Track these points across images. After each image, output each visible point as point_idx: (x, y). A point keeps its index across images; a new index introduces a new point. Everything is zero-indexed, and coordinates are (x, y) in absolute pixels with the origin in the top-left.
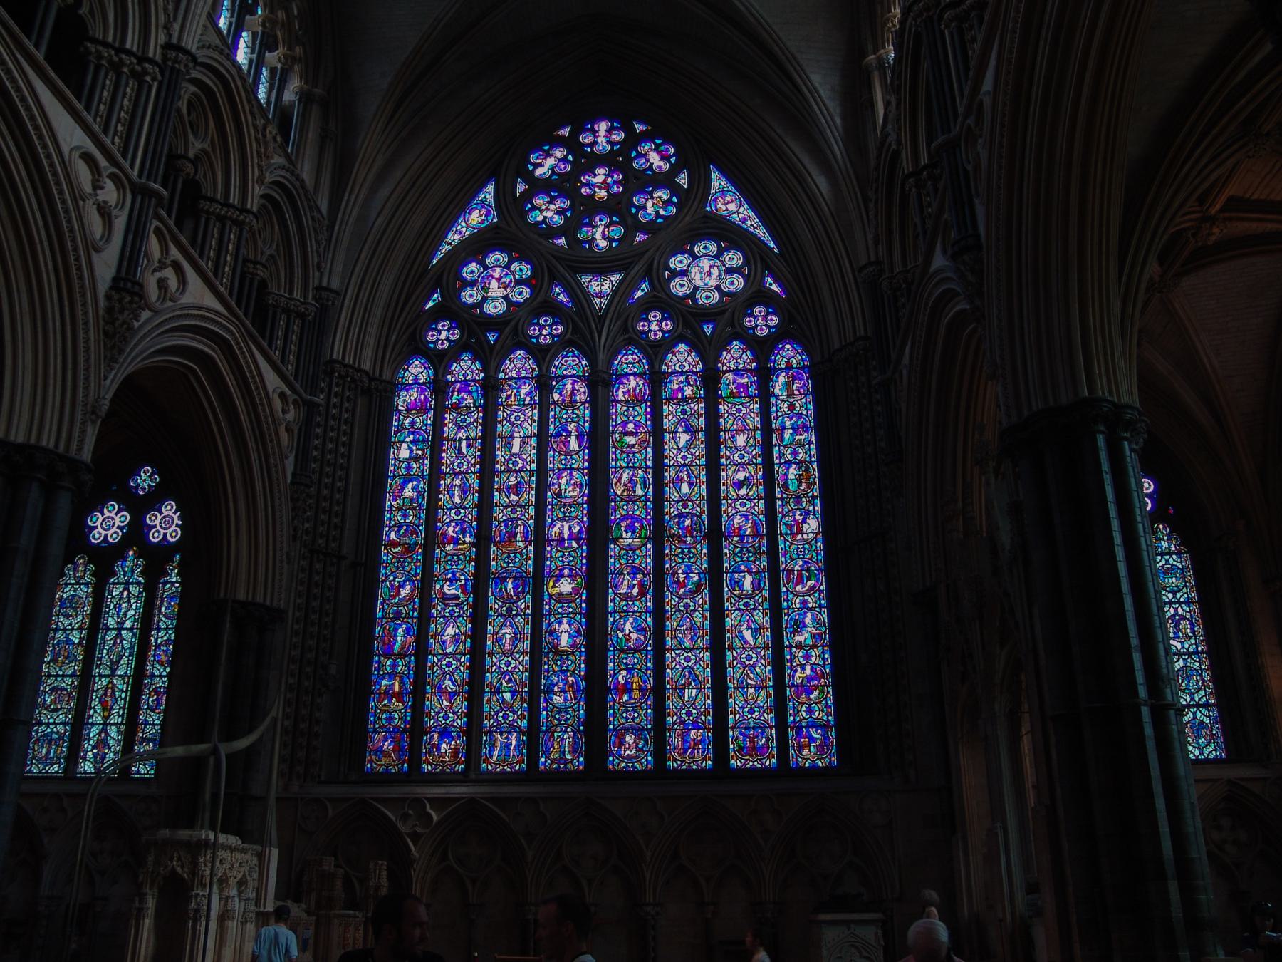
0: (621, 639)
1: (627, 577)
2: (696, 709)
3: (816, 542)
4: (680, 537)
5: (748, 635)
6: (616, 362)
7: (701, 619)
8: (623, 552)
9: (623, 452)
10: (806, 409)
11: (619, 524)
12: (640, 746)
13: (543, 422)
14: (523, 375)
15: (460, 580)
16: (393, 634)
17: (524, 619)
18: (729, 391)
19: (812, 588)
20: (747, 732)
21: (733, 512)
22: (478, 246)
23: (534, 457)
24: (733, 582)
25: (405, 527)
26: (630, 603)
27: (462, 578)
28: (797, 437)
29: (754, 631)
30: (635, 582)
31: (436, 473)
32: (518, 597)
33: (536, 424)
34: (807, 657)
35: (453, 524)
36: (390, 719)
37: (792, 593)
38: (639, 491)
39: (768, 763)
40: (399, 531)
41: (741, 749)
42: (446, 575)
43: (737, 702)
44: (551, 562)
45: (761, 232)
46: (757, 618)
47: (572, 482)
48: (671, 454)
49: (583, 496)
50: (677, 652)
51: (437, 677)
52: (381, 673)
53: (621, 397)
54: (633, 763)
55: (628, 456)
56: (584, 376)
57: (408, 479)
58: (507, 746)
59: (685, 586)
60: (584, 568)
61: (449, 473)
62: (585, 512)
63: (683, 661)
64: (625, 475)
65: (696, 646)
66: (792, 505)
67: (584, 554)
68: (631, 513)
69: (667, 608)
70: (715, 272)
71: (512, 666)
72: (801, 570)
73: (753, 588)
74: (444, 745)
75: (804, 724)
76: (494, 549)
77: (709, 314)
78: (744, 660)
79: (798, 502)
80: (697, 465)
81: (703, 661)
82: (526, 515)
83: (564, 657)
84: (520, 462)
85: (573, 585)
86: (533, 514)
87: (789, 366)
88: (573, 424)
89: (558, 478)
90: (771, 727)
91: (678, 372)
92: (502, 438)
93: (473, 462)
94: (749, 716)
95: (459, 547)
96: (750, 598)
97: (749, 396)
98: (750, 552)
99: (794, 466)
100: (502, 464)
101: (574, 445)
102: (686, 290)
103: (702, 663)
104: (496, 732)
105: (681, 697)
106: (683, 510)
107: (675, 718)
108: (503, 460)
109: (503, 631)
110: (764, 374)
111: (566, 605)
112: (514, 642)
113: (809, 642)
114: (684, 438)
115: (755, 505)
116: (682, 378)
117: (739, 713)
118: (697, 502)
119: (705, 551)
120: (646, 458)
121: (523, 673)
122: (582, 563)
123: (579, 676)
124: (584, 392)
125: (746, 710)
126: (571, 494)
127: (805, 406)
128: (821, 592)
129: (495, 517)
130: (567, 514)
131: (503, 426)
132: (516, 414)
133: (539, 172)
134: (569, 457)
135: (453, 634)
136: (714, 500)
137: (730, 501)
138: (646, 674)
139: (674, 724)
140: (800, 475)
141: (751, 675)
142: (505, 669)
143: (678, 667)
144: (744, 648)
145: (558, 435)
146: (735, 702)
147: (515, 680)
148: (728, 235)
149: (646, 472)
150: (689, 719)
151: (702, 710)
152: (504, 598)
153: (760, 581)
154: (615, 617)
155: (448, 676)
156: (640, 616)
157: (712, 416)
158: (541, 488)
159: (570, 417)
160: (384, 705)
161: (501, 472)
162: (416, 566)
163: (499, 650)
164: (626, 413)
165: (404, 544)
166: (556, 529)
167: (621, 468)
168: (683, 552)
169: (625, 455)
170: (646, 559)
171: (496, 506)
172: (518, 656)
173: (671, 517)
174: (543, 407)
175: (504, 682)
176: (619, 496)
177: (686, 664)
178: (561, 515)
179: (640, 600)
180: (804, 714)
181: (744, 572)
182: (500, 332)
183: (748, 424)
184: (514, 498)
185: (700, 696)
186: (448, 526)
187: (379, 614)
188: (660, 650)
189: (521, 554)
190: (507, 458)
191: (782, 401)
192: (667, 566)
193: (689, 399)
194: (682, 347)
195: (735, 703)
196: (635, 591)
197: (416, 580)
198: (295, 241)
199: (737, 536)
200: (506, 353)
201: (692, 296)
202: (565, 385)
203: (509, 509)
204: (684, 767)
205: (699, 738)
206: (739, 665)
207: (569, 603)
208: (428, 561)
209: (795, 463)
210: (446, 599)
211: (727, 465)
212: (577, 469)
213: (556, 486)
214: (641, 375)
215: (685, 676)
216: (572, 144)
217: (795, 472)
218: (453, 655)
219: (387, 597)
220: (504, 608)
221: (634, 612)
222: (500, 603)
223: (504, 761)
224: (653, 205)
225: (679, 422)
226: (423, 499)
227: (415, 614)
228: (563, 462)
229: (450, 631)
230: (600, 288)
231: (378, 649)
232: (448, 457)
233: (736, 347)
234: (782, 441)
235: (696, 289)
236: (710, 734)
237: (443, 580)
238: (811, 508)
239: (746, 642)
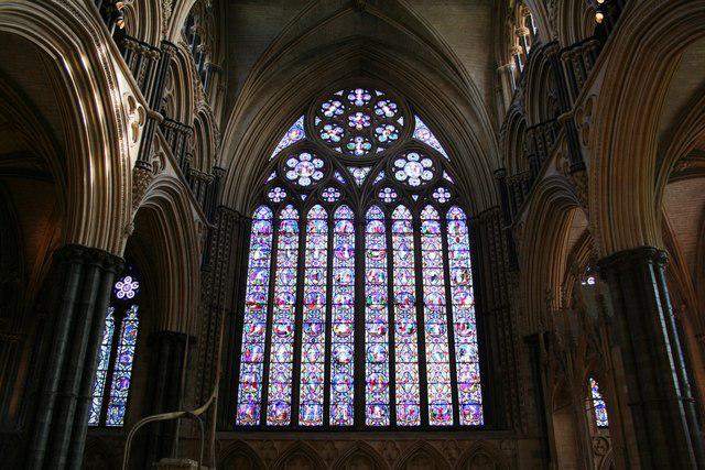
5: (437, 356)
7: (414, 348)
13: (330, 242)
16: (250, 352)
22: (296, 150)
31: (273, 268)
36: (250, 397)
38: (381, 280)
45: (441, 150)
53: (370, 231)
57: (259, 269)
58: (312, 413)
70: (418, 169)
77: (415, 190)
101: (346, 255)
102: (404, 178)
110: (444, 222)
113: (469, 360)
114: (403, 254)
127: (465, 239)
133: (327, 113)
136: (419, 286)
145: (338, 249)
146: (432, 390)
148: (424, 151)
157: (418, 243)
158: (330, 277)
174: (330, 235)
182: (308, 195)
184: (315, 282)
188: (392, 363)
194: (401, 207)
196: (379, 332)
198: (205, 143)
200: (310, 206)
201: (407, 181)
208: (270, 313)
210: (279, 334)
216: (344, 100)
224: (385, 134)
230: (359, 175)
232: (280, 259)
233: (429, 208)
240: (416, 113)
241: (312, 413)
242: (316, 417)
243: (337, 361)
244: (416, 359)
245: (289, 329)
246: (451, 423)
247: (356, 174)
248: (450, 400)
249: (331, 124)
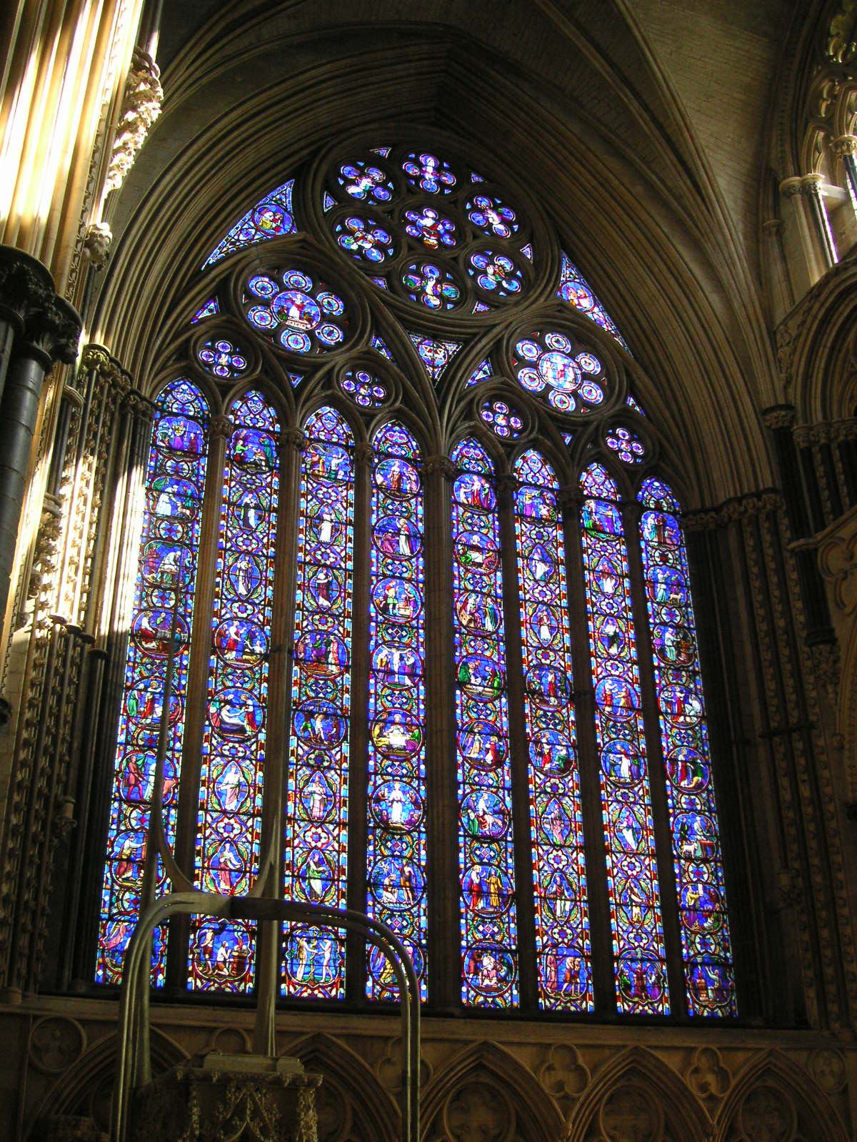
0: (473, 821)
1: (477, 737)
2: (571, 928)
3: (701, 728)
4: (542, 694)
5: (628, 835)
6: (455, 453)
8: (472, 703)
9: (467, 570)
10: (681, 563)
11: (465, 664)
12: (503, 974)
13: (361, 507)
14: (334, 440)
15: (245, 704)
17: (340, 776)
18: (591, 522)
19: (698, 786)
20: (634, 965)
21: (604, 674)
23: (350, 552)
24: (608, 764)
25: (163, 615)
26: (483, 773)
27: (250, 702)
28: (672, 596)
29: (635, 832)
30: (488, 746)
32: (331, 743)
33: (352, 509)
34: (699, 873)
35: (236, 623)
37: (676, 788)
38: (489, 626)
39: (660, 1009)
40: (155, 618)
41: (627, 987)
42: (225, 695)
43: (621, 924)
44: (376, 700)
46: (638, 816)
47: (403, 596)
48: (526, 586)
49: (417, 618)
50: (545, 848)
51: (211, 845)
52: (123, 828)
53: (462, 498)
54: (494, 997)
55: (474, 577)
56: (415, 460)
58: (317, 962)
59: (551, 761)
60: (422, 715)
61: (229, 549)
62: (421, 640)
63: (552, 862)
64: (471, 601)
65: (568, 843)
66: (671, 678)
67: (422, 697)
68: (479, 652)
69: (531, 786)
70: (570, 375)
71: (323, 841)
72: (686, 762)
73: (632, 775)
74: (222, 950)
75: (699, 960)
76: (296, 668)
78: (626, 869)
79: (678, 677)
80: (557, 605)
81: (577, 864)
82: (341, 629)
83: (397, 837)
84: (332, 555)
85: (408, 737)
86: (350, 629)
87: (658, 508)
88: (403, 521)
89: (384, 588)
90: (661, 960)
91: (530, 484)
92: (306, 517)
93: (265, 540)
94: (636, 944)
95: (245, 657)
96: (628, 788)
97: (615, 534)
98: (626, 729)
99: (671, 630)
100: (307, 553)
101: (404, 548)
102: (536, 386)
103: (575, 867)
104: (301, 937)
105: (553, 911)
106: (543, 661)
107: (545, 938)
108: (308, 547)
109: (310, 789)
111: (397, 763)
112: (325, 806)
113: (699, 854)
114: (541, 569)
115: (628, 670)
116: (536, 493)
117: (623, 939)
118: (561, 653)
119: (572, 718)
120: (495, 583)
121: (339, 853)
122: (418, 708)
123: (419, 866)
124: (416, 482)
125: (632, 935)
126: (402, 612)
128: (709, 792)
129: (298, 625)
130: (396, 639)
131: (308, 502)
132: (325, 490)
134: (397, 562)
135: (236, 782)
136: (580, 653)
137: (599, 660)
138: (506, 874)
139: (545, 946)
140: (678, 643)
141: (636, 890)
142: (313, 844)
143: (546, 868)
144: (625, 853)
145: (383, 530)
146: (618, 924)
147: (329, 863)
149: (496, 602)
150: (563, 942)
151: (579, 930)
152: (311, 740)
153: (639, 767)
154: (464, 790)
155: (228, 846)
156: (496, 793)
158: (361, 596)
159: (397, 510)
160: (127, 879)
161: (305, 563)
162: (180, 674)
163: (305, 816)
164: (469, 521)
165: (161, 639)
166: (382, 656)
167: (466, 590)
168: (545, 715)
169: (470, 575)
170: (501, 716)
171: (299, 608)
172: (331, 827)
173: (530, 668)
174: (361, 485)
175: (312, 864)
176: (465, 627)
177: (556, 866)
178: (388, 638)
179: (494, 770)
180: (699, 946)
181: (621, 753)
183: (615, 568)
185: (575, 911)
186: (229, 626)
187: (121, 738)
188: (523, 847)
189: (333, 681)
190: (313, 545)
191: (653, 548)
192: (528, 730)
193: (546, 520)
194: (532, 454)
195: (618, 925)
196: (489, 758)
197: (180, 695)
199: (609, 706)
202: (391, 466)
203: (317, 617)
204: (560, 1008)
205: (577, 968)
206: (620, 875)
207: (401, 761)
208: (199, 672)
209: (671, 627)
210: (225, 731)
211: (594, 614)
212: (409, 580)
213: (381, 598)
214: (486, 477)
215: (555, 882)
217: (672, 638)
218: (236, 814)
219: (134, 714)
220: (312, 756)
221: (491, 786)
222: (306, 748)
223: (314, 981)
225: (533, 548)
226: (192, 580)
227: (178, 745)
228: (390, 567)
229: (232, 777)
230: (435, 355)
231: (118, 791)
234: (655, 597)
235: (549, 387)
236: (589, 965)
237: (220, 702)
238: (692, 686)
239: (627, 845)
240: (565, 246)
241: (317, 962)
242: (327, 973)
243: (384, 824)
244: (577, 839)
245: (252, 721)
246: (664, 1008)
247: (425, 353)
248: (660, 947)
249: (363, 219)
